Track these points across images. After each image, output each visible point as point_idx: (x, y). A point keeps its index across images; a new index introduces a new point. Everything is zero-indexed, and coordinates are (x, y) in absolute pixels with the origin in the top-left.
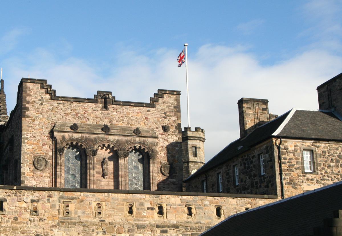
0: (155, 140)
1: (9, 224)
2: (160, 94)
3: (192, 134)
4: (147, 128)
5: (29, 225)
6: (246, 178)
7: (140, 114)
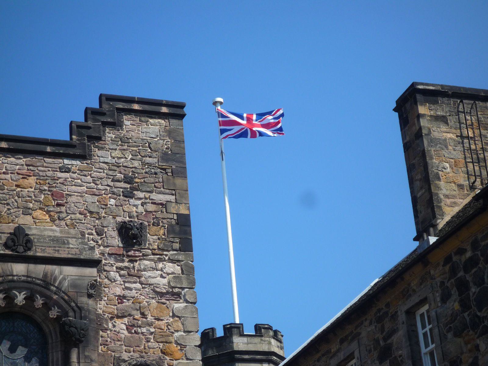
0: (92, 271)
2: (109, 112)
3: (248, 343)
4: (58, 229)
6: (477, 347)
7: (32, 180)
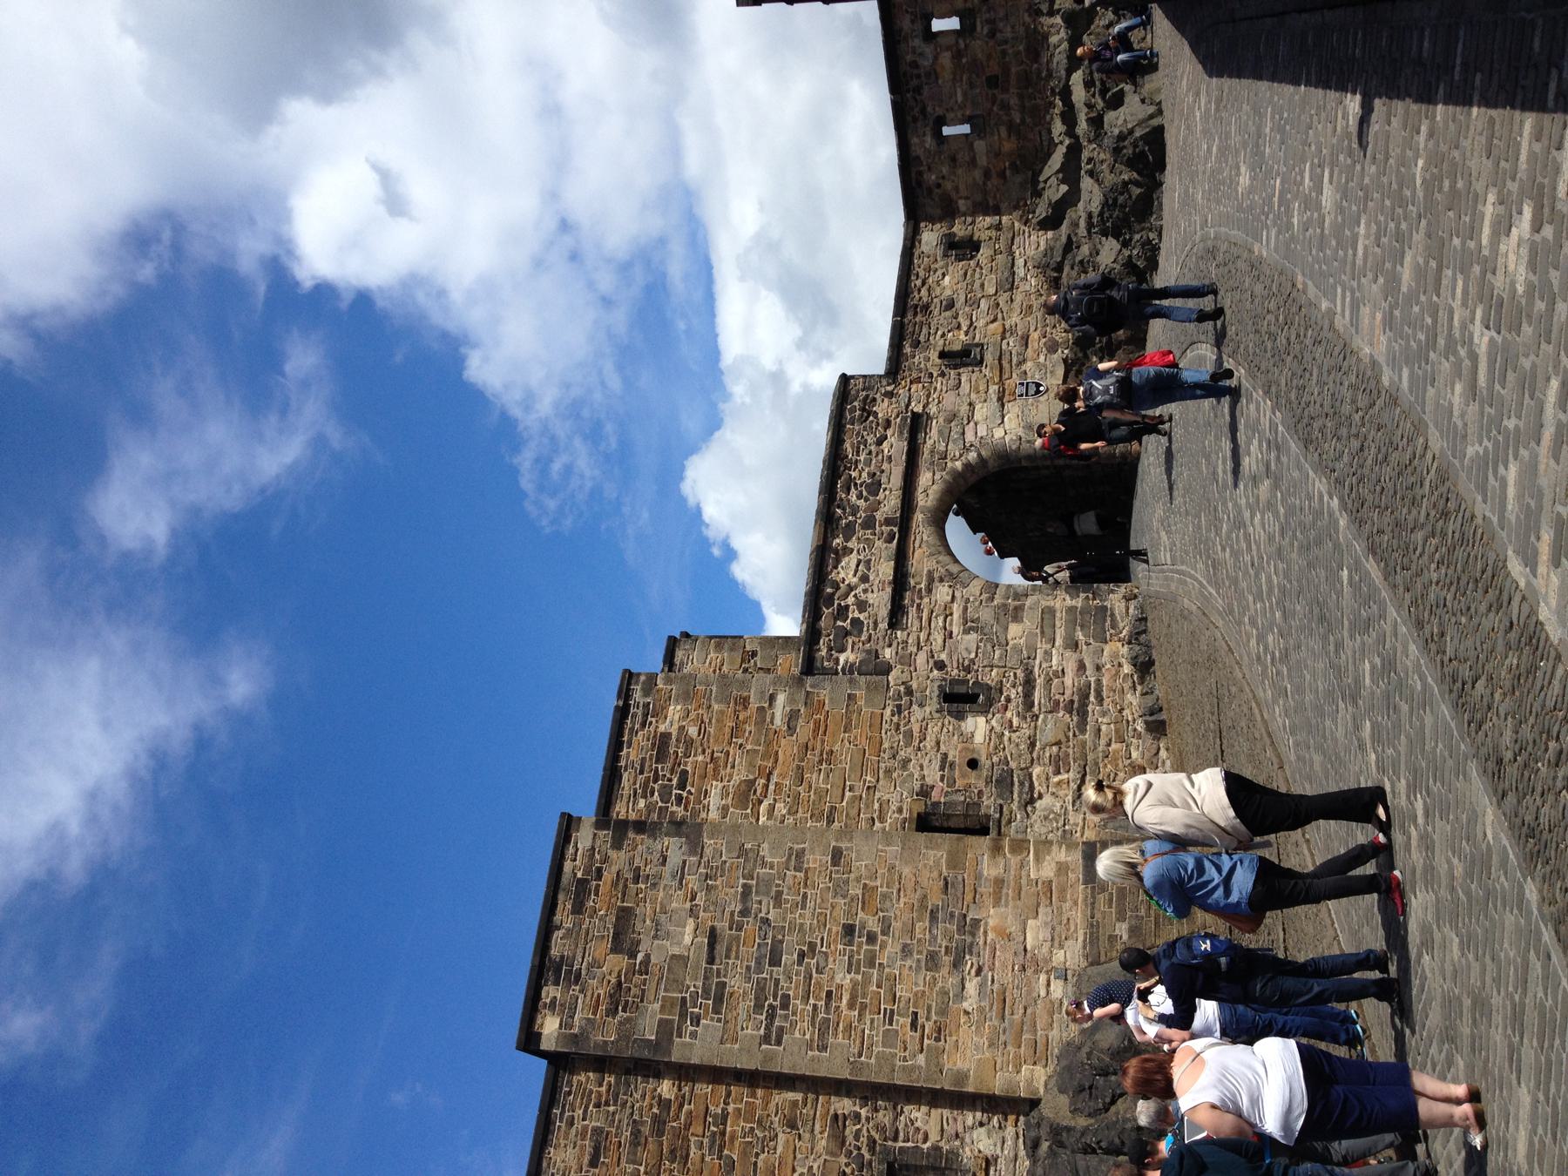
1: (1014, 101)
5: (1009, 35)
